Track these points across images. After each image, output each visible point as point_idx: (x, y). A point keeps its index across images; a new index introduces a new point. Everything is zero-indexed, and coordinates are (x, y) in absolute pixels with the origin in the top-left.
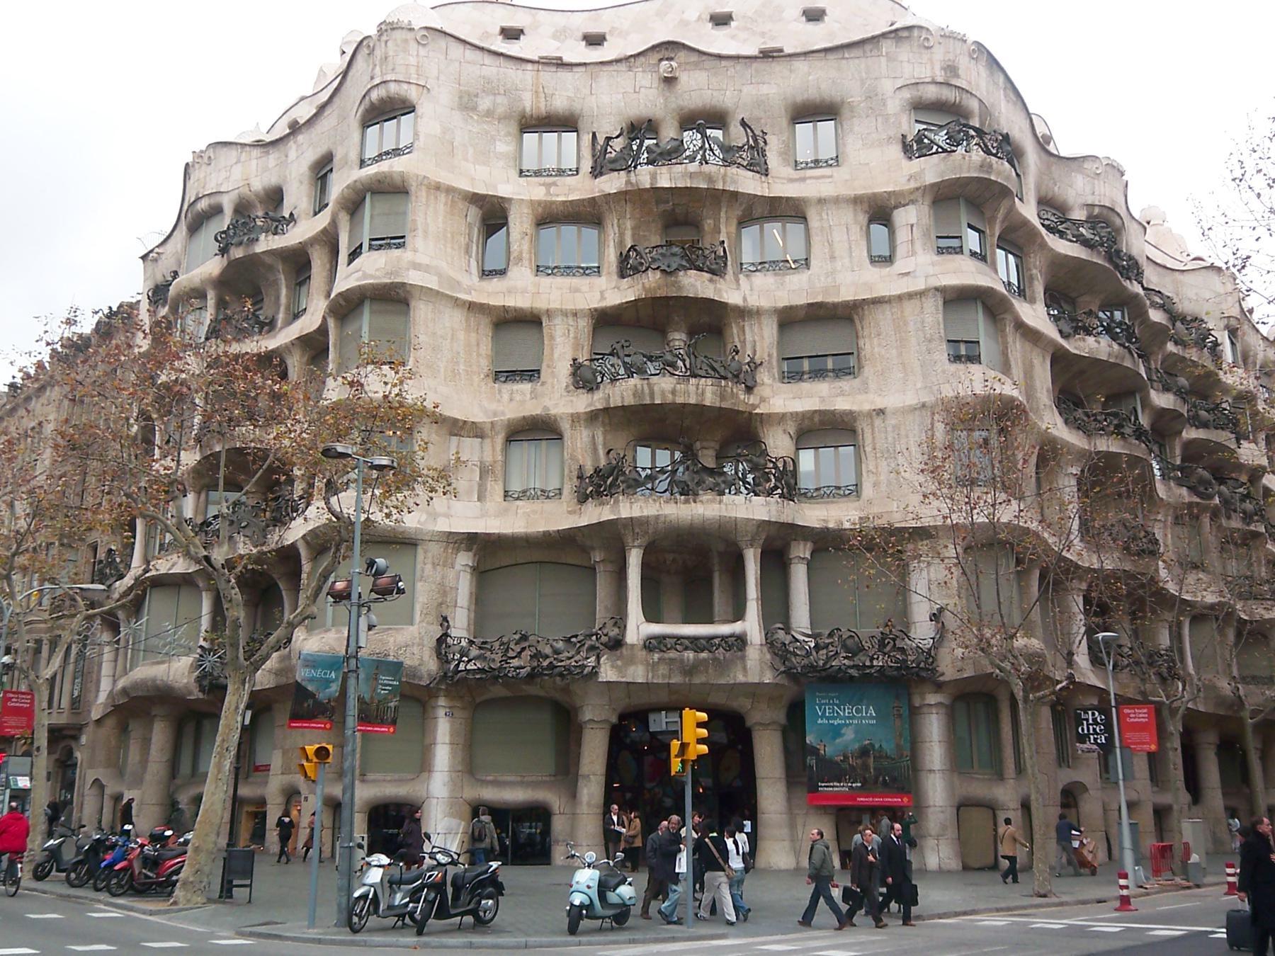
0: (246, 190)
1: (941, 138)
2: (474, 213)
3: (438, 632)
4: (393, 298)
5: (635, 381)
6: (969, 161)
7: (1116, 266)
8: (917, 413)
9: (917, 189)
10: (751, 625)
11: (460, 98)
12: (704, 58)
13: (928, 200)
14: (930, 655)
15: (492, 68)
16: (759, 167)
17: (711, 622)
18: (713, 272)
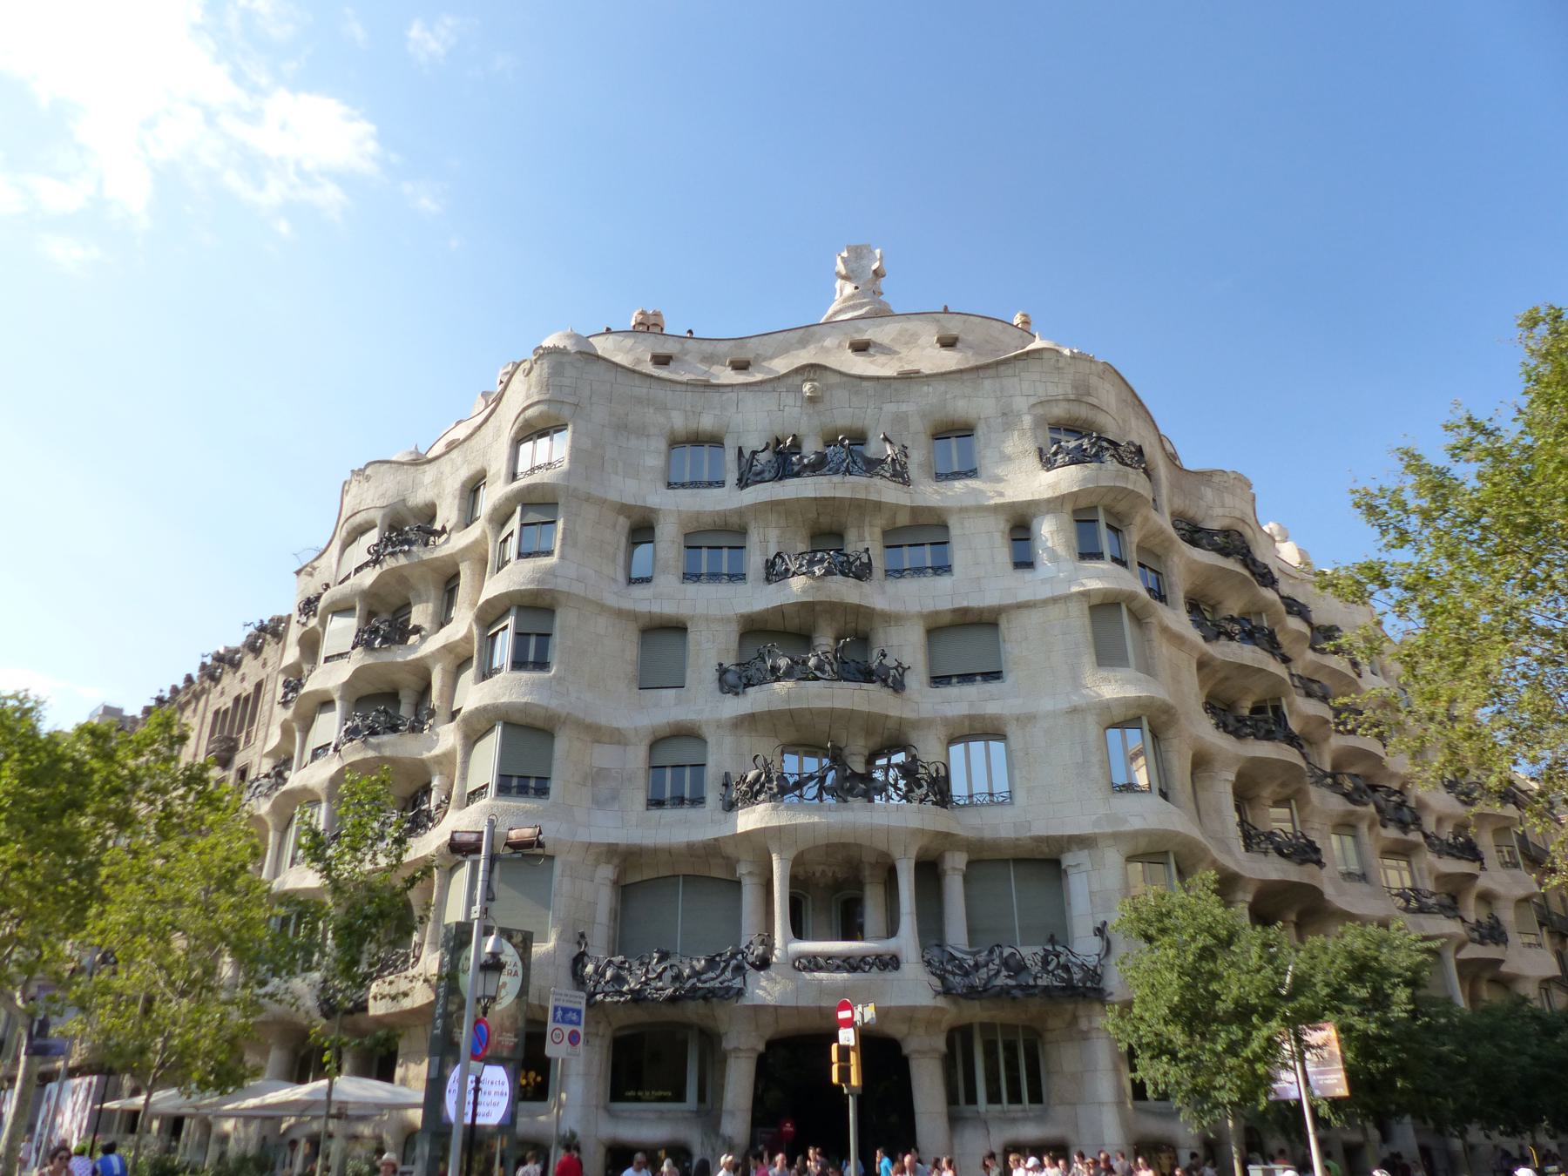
2: (623, 524)
3: (576, 951)
7: (1253, 574)
13: (1069, 508)
15: (642, 390)
17: (863, 939)
18: (858, 577)
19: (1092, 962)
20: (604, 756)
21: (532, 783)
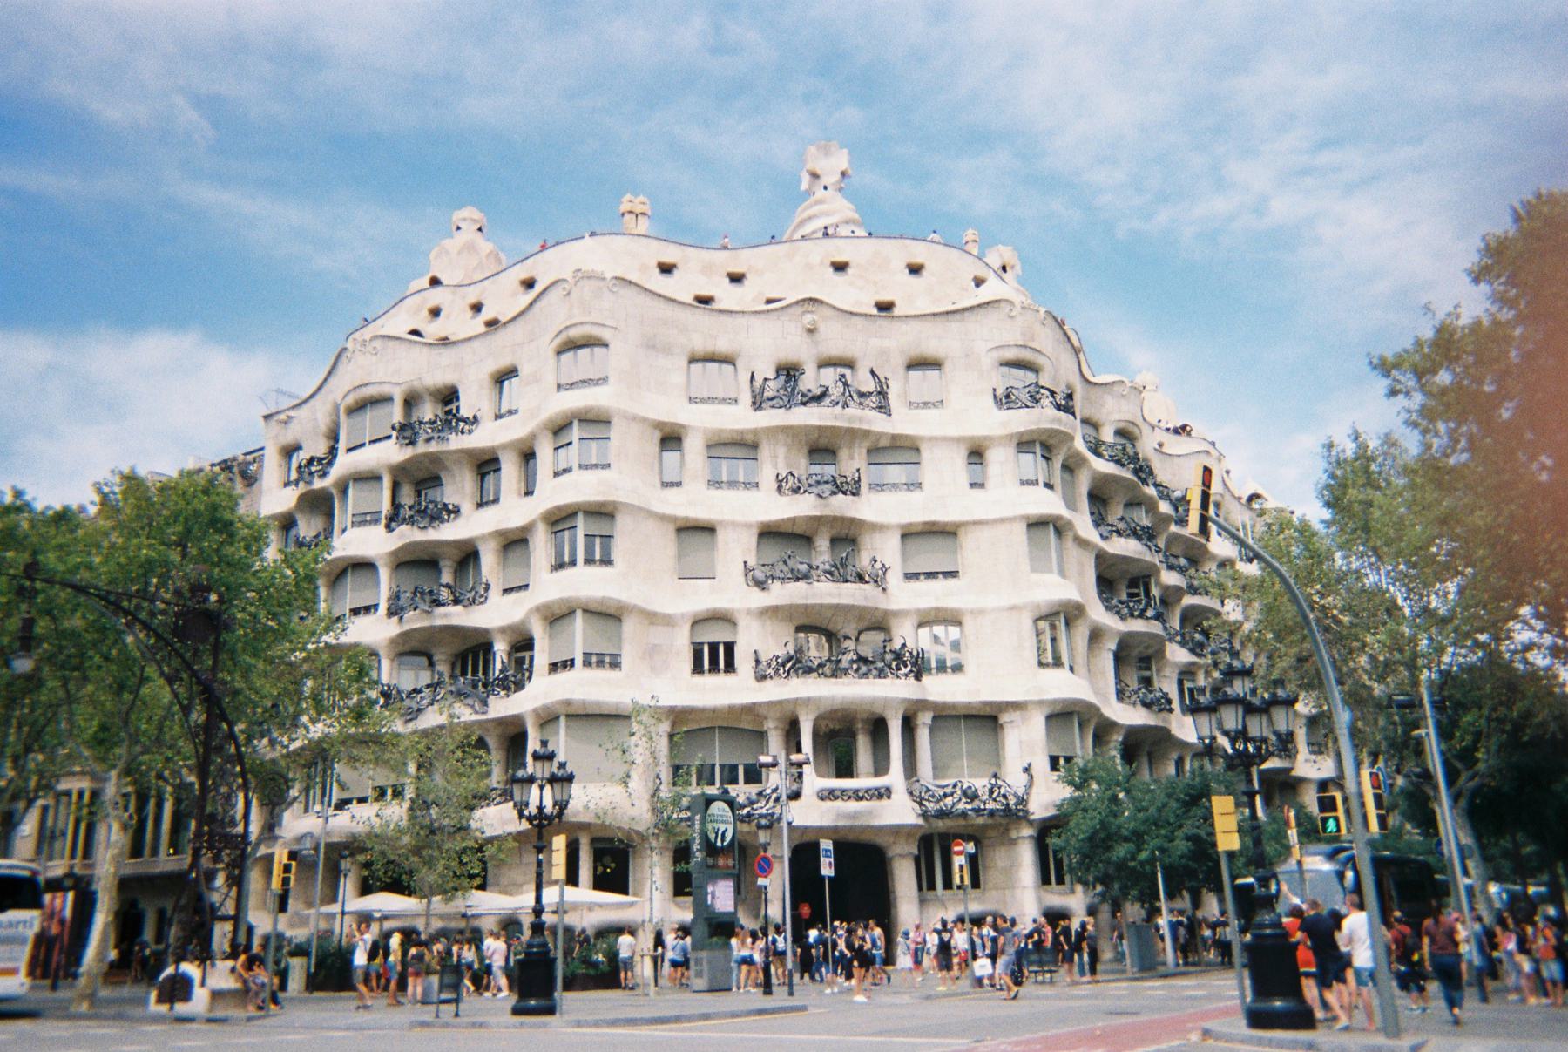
0: (416, 384)
1: (1024, 397)
2: (658, 435)
4: (602, 513)
5: (802, 584)
6: (1045, 417)
10: (895, 776)
13: (1015, 441)
14: (1022, 801)
16: (884, 408)
18: (853, 494)
19: (1021, 792)
20: (658, 635)
21: (607, 659)
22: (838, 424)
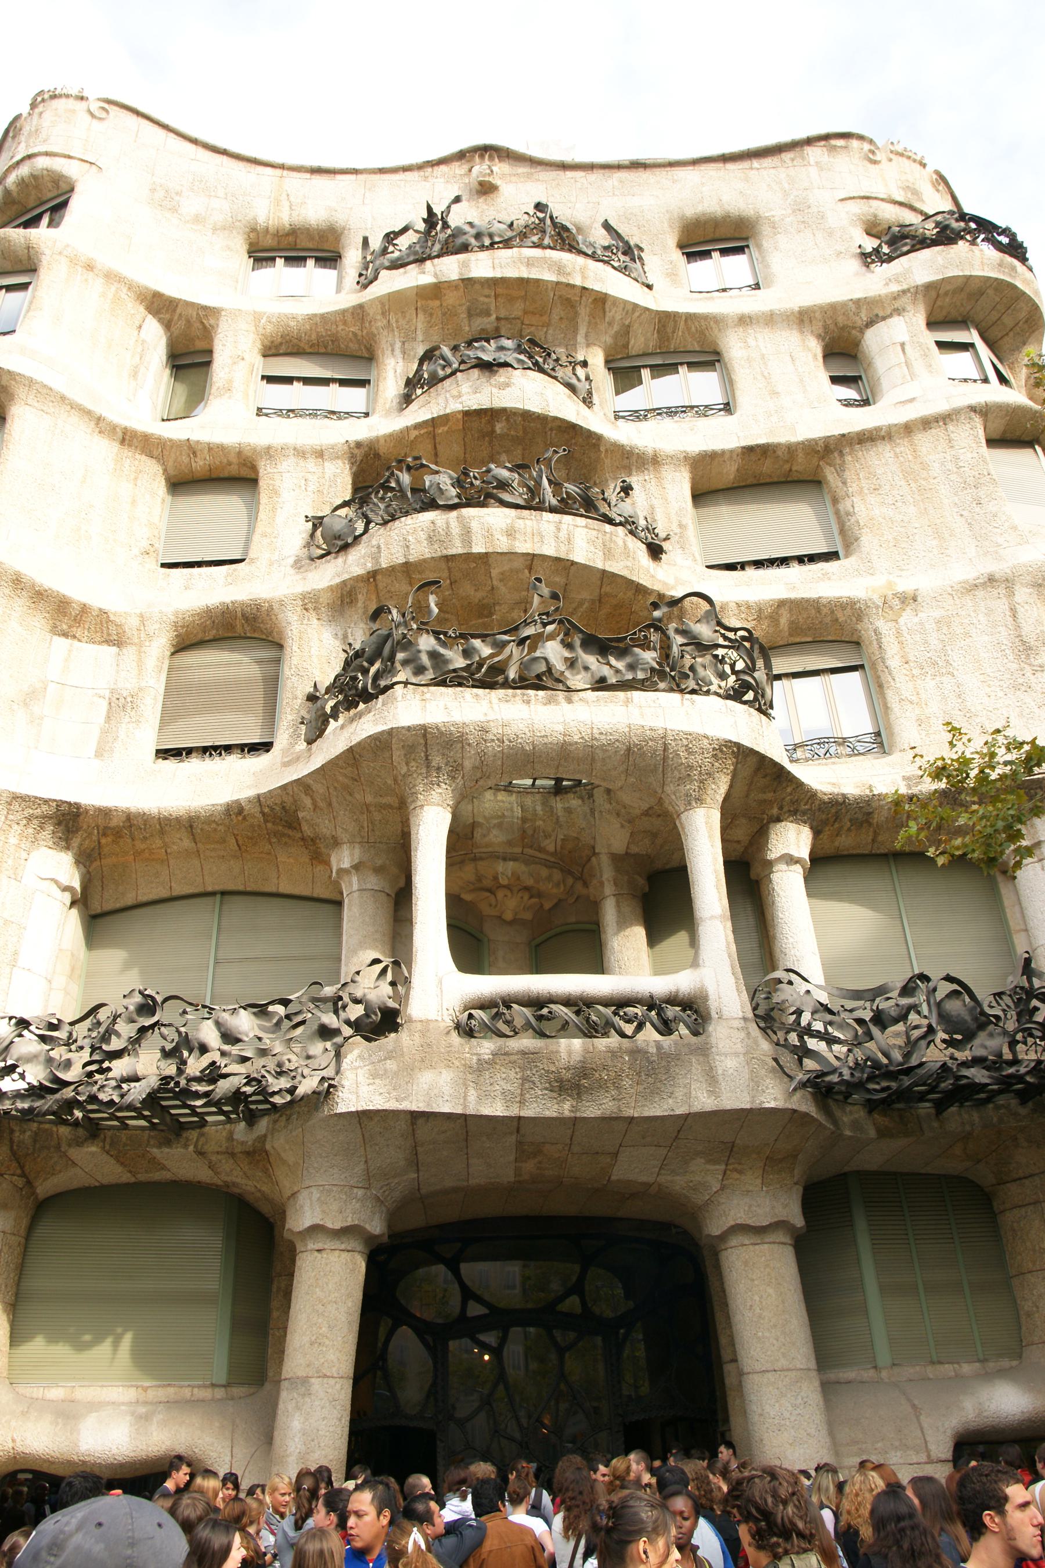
8: (980, 593)
9: (904, 292)
11: (153, 190)
12: (539, 168)
22: (534, 274)
